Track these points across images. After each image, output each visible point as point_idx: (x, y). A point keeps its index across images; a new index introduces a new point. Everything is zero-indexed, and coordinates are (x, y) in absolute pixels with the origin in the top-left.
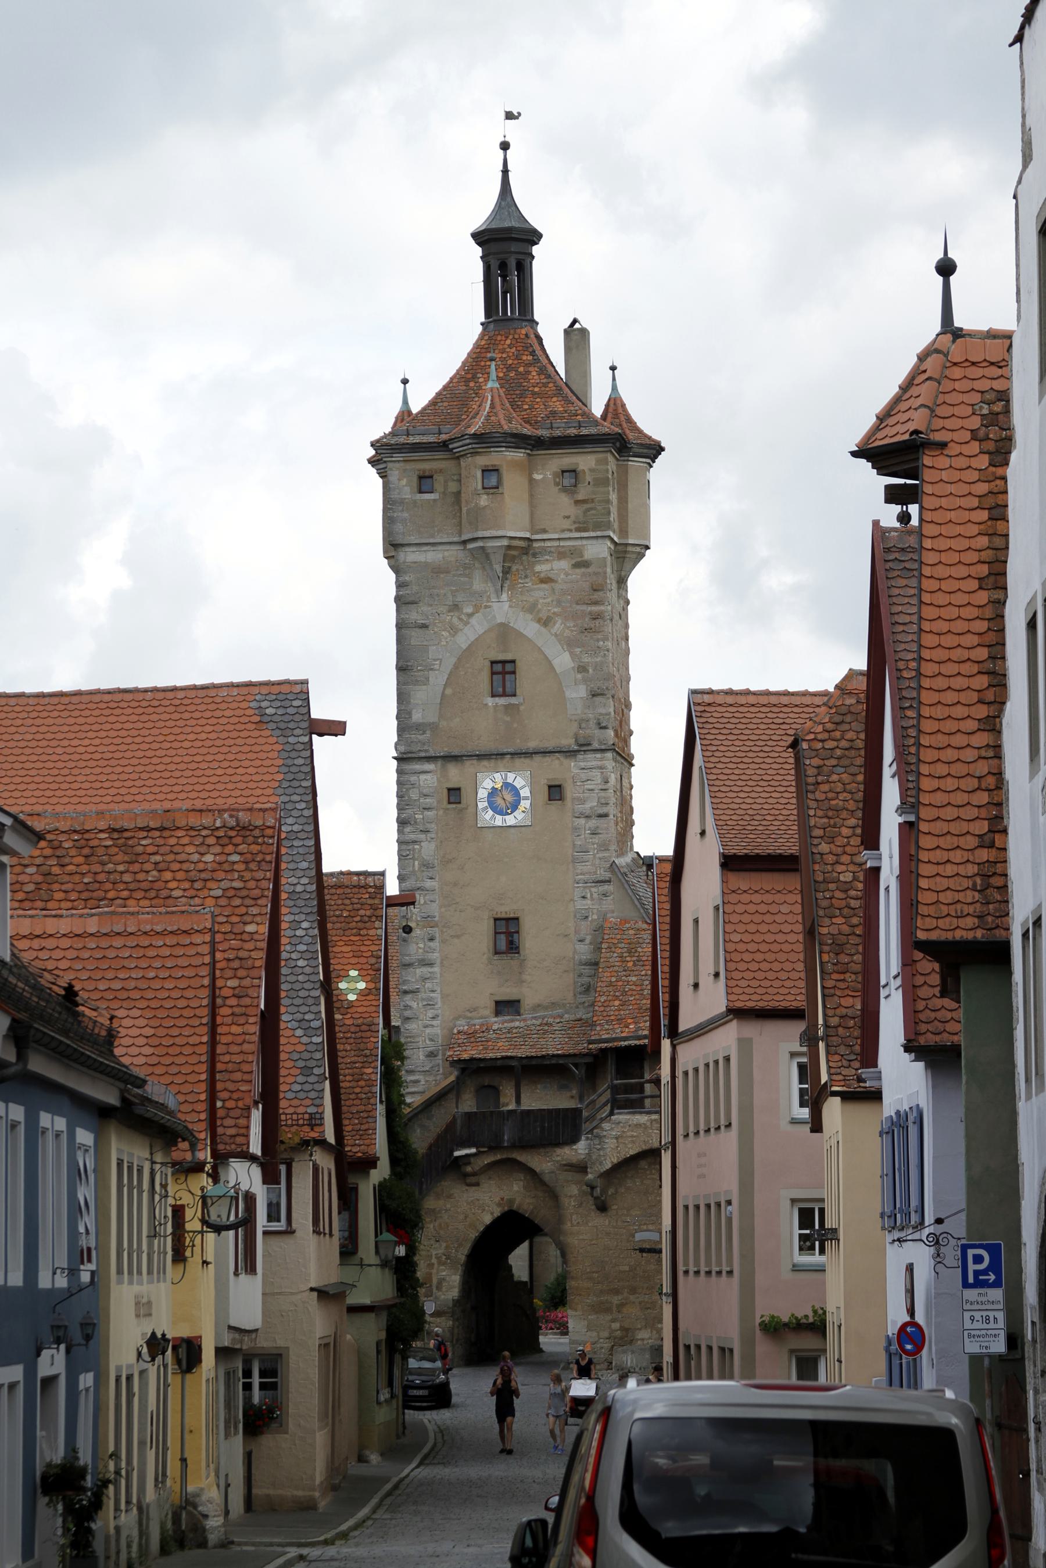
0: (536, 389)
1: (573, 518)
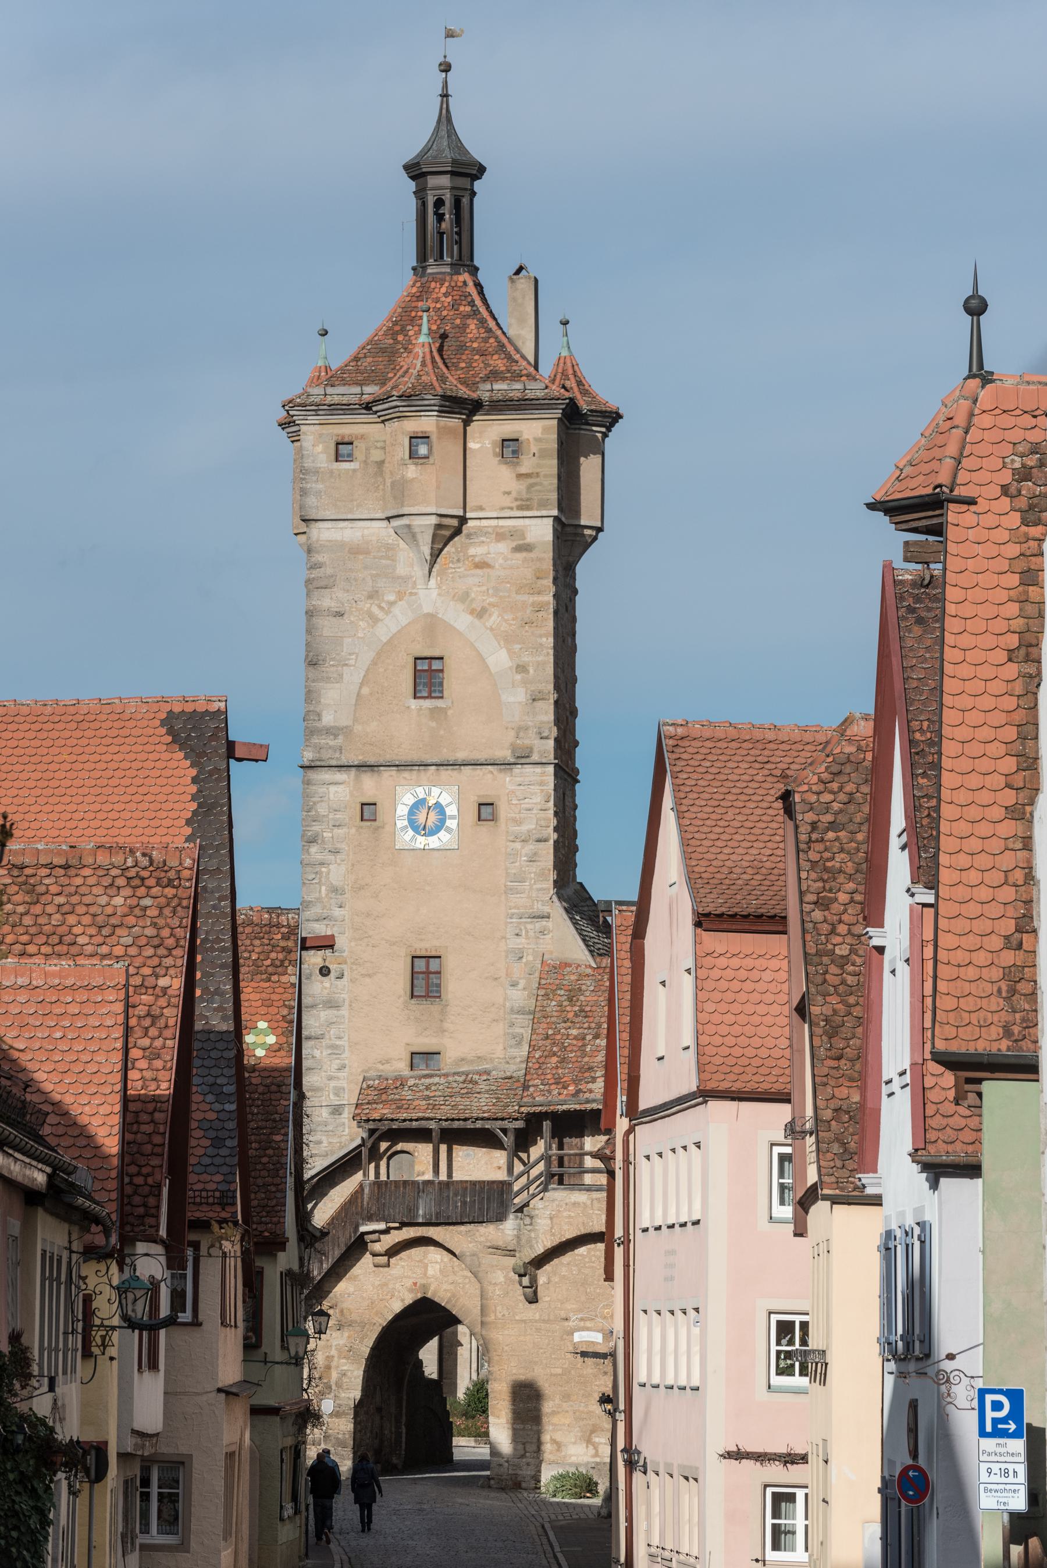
0: (475, 345)
1: (514, 494)
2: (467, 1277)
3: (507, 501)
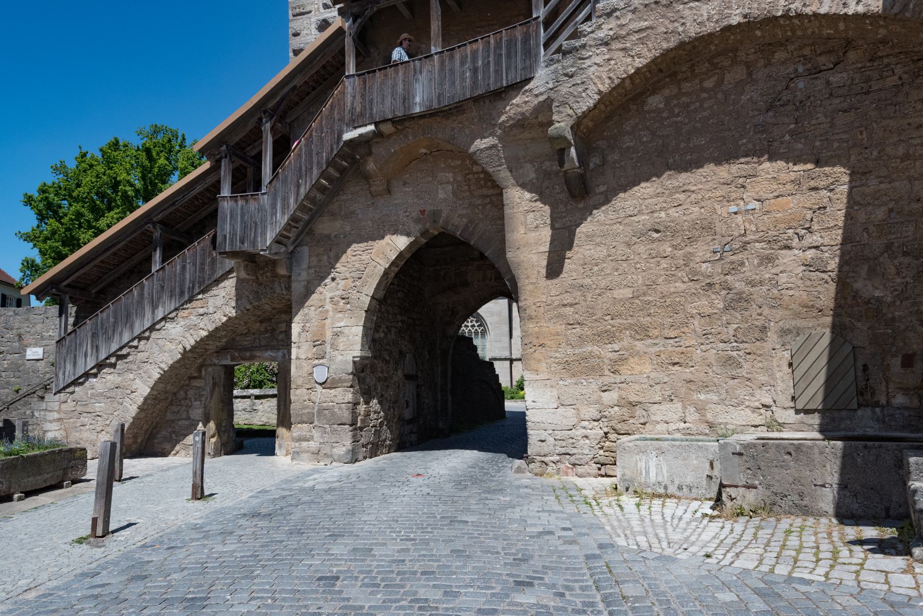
2: (487, 196)
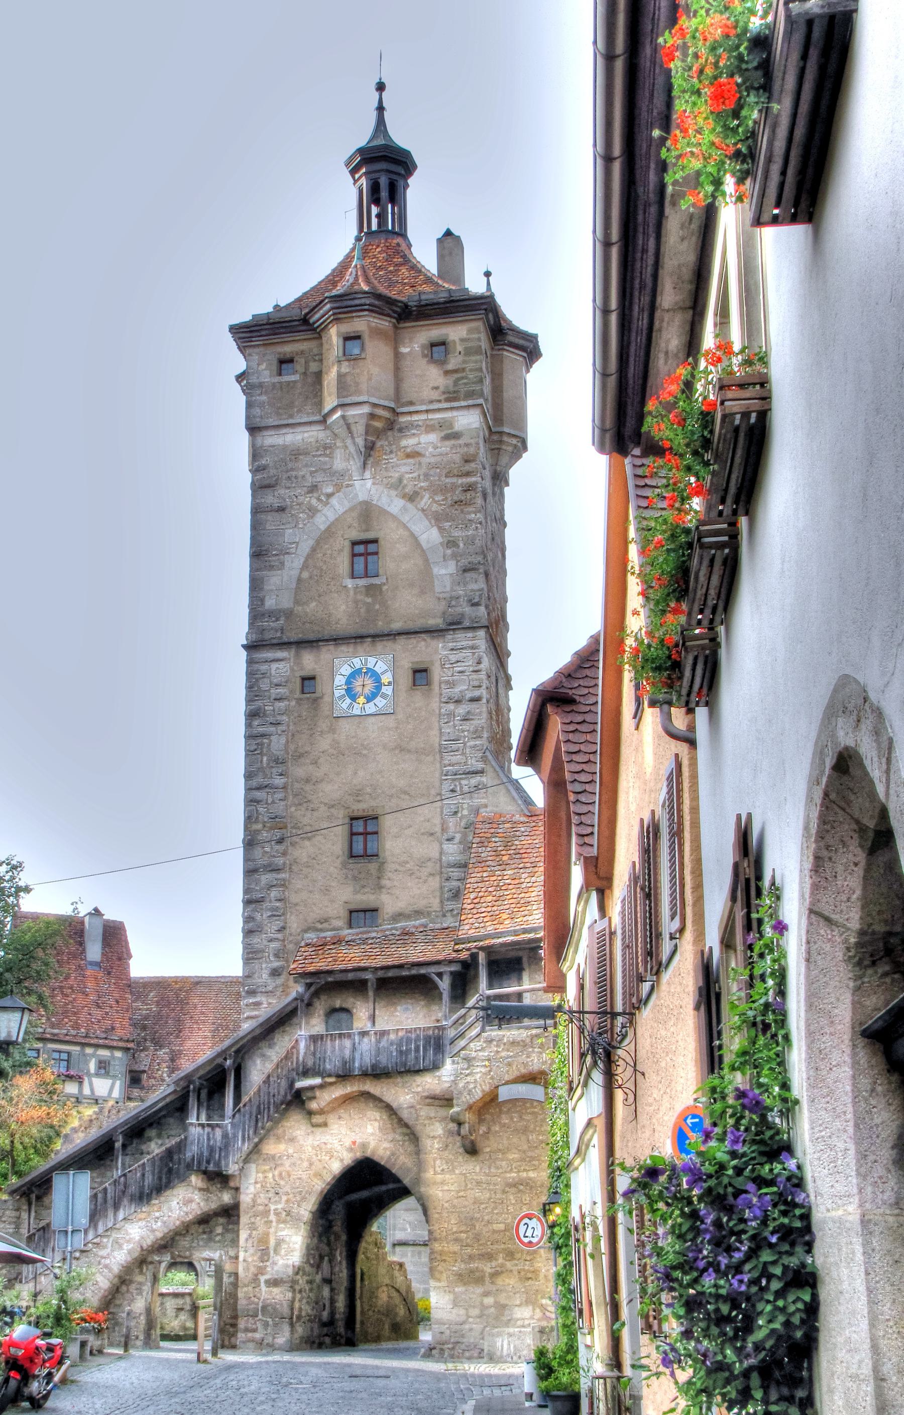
1: (442, 389)
3: (435, 395)
